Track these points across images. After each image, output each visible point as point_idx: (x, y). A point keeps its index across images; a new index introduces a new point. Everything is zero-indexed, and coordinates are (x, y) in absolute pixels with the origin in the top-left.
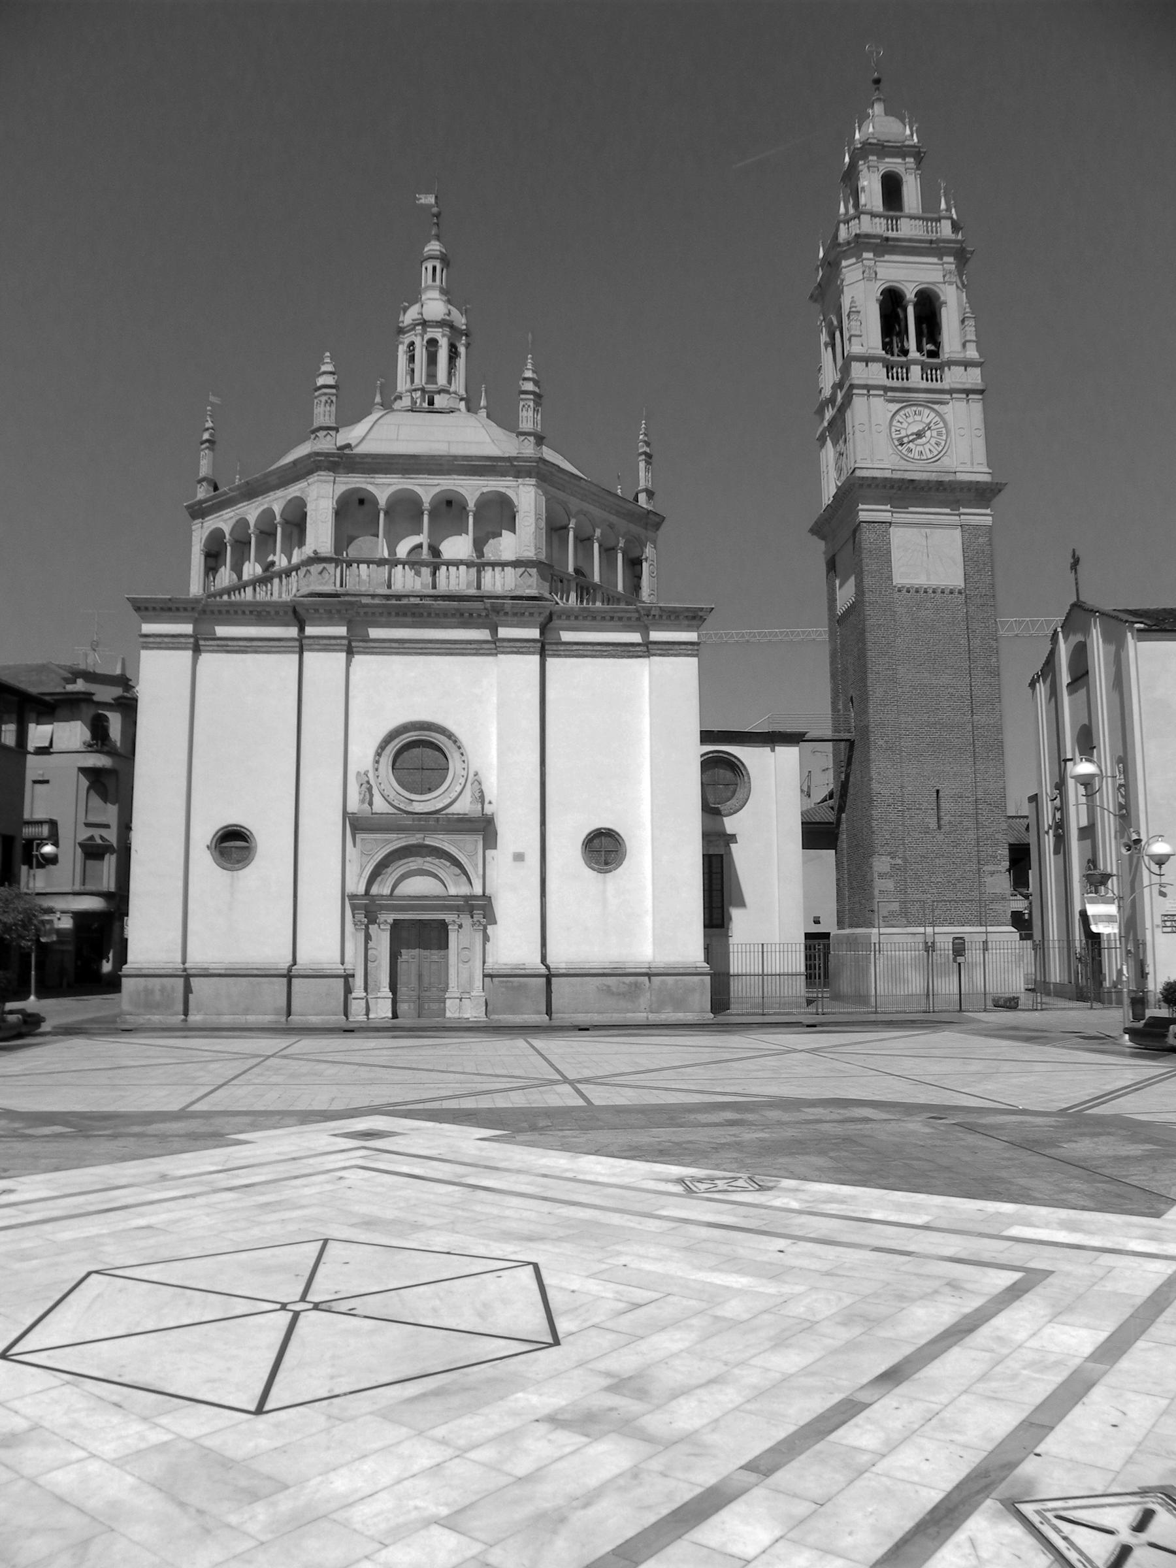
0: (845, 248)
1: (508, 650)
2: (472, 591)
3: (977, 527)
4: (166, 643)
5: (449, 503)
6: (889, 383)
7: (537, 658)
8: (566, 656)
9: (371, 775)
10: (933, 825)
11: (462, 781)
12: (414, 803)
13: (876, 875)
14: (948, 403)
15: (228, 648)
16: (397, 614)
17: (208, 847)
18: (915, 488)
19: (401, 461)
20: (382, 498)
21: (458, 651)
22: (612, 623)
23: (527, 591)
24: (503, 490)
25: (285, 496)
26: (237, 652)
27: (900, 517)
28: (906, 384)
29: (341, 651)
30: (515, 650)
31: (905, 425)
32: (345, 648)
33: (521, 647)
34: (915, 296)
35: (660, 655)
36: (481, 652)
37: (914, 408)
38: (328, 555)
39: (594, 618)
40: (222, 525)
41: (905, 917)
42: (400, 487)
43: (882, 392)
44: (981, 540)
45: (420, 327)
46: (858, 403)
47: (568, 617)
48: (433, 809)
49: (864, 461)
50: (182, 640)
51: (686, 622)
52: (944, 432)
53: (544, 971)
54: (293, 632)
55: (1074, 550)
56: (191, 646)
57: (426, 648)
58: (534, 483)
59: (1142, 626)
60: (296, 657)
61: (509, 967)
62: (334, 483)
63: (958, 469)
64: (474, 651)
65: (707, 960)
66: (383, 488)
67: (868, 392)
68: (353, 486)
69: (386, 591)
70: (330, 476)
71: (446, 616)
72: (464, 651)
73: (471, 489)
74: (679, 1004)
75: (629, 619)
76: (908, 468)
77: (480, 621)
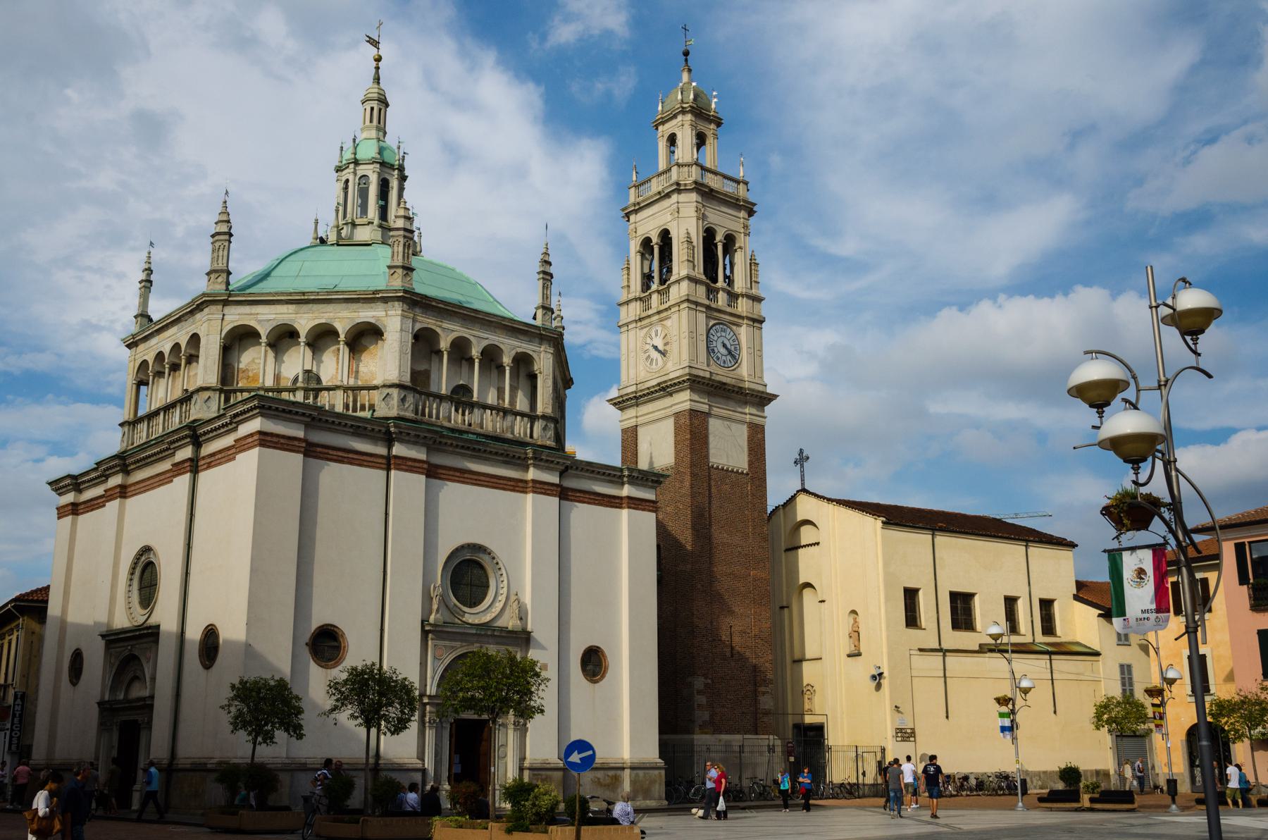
0: (682, 188)
1: (539, 490)
2: (509, 436)
4: (282, 444)
7: (557, 499)
10: (728, 654)
11: (502, 598)
12: (466, 614)
13: (695, 692)
14: (741, 326)
15: (329, 456)
16: (463, 447)
17: (307, 644)
18: (725, 389)
19: (465, 312)
21: (501, 486)
22: (603, 477)
24: (531, 353)
25: (353, 318)
27: (715, 411)
29: (421, 473)
30: (543, 491)
31: (716, 338)
32: (425, 471)
33: (548, 489)
34: (725, 239)
35: (634, 508)
36: (517, 489)
37: (721, 326)
38: (409, 384)
39: (593, 471)
40: (253, 323)
41: (715, 727)
42: (460, 334)
44: (759, 436)
45: (378, 166)
47: (577, 468)
48: (482, 622)
49: (692, 362)
50: (296, 443)
51: (650, 484)
54: (381, 450)
55: (801, 451)
56: (303, 450)
57: (479, 480)
58: (552, 352)
59: (884, 519)
60: (385, 472)
61: (539, 762)
62: (414, 321)
63: (746, 379)
64: (512, 488)
65: (660, 757)
66: (448, 333)
68: (426, 326)
70: (410, 313)
71: (496, 454)
72: (505, 487)
73: (510, 347)
74: (647, 794)
76: (719, 373)
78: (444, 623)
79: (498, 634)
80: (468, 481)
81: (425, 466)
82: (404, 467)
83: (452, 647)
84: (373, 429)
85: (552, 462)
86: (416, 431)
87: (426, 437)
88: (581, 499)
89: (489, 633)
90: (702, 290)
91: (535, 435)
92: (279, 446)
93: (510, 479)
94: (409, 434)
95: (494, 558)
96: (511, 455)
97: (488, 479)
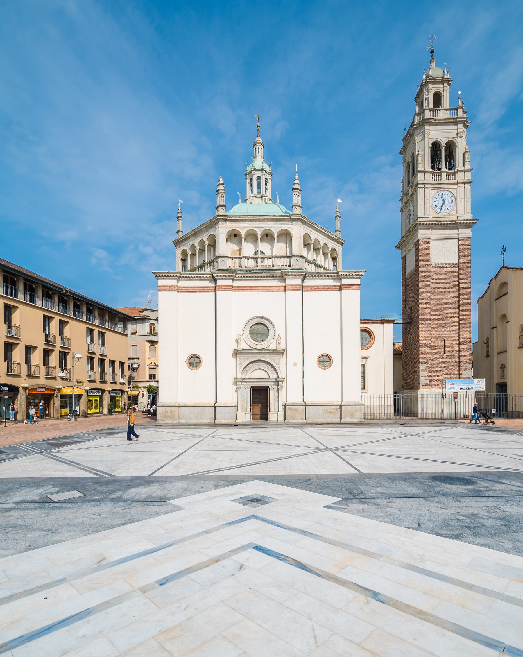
1: (290, 289)
2: (276, 268)
3: (465, 238)
5: (267, 235)
6: (433, 182)
8: (311, 291)
9: (241, 335)
16: (250, 277)
20: (243, 234)
23: (297, 267)
26: (193, 292)
28: (440, 182)
30: (292, 289)
36: (280, 290)
37: (442, 192)
39: (321, 276)
43: (429, 186)
46: (420, 191)
51: (355, 276)
52: (454, 200)
53: (304, 404)
60: (214, 293)
64: (278, 290)
67: (424, 186)
69: (246, 269)
71: (267, 276)
72: (274, 290)
75: (334, 276)
77: (280, 278)
78: (243, 349)
79: (268, 352)
80: (255, 290)
81: (231, 287)
82: (222, 289)
83: (248, 359)
84: (206, 277)
85: (295, 275)
86: (224, 273)
87: (229, 276)
88: (316, 289)
89: (264, 352)
90: (429, 177)
91: (291, 266)
92: (166, 290)
93: (276, 287)
94: (221, 276)
95: (269, 321)
96: (275, 276)
97: (264, 288)
